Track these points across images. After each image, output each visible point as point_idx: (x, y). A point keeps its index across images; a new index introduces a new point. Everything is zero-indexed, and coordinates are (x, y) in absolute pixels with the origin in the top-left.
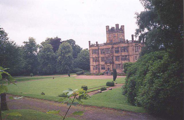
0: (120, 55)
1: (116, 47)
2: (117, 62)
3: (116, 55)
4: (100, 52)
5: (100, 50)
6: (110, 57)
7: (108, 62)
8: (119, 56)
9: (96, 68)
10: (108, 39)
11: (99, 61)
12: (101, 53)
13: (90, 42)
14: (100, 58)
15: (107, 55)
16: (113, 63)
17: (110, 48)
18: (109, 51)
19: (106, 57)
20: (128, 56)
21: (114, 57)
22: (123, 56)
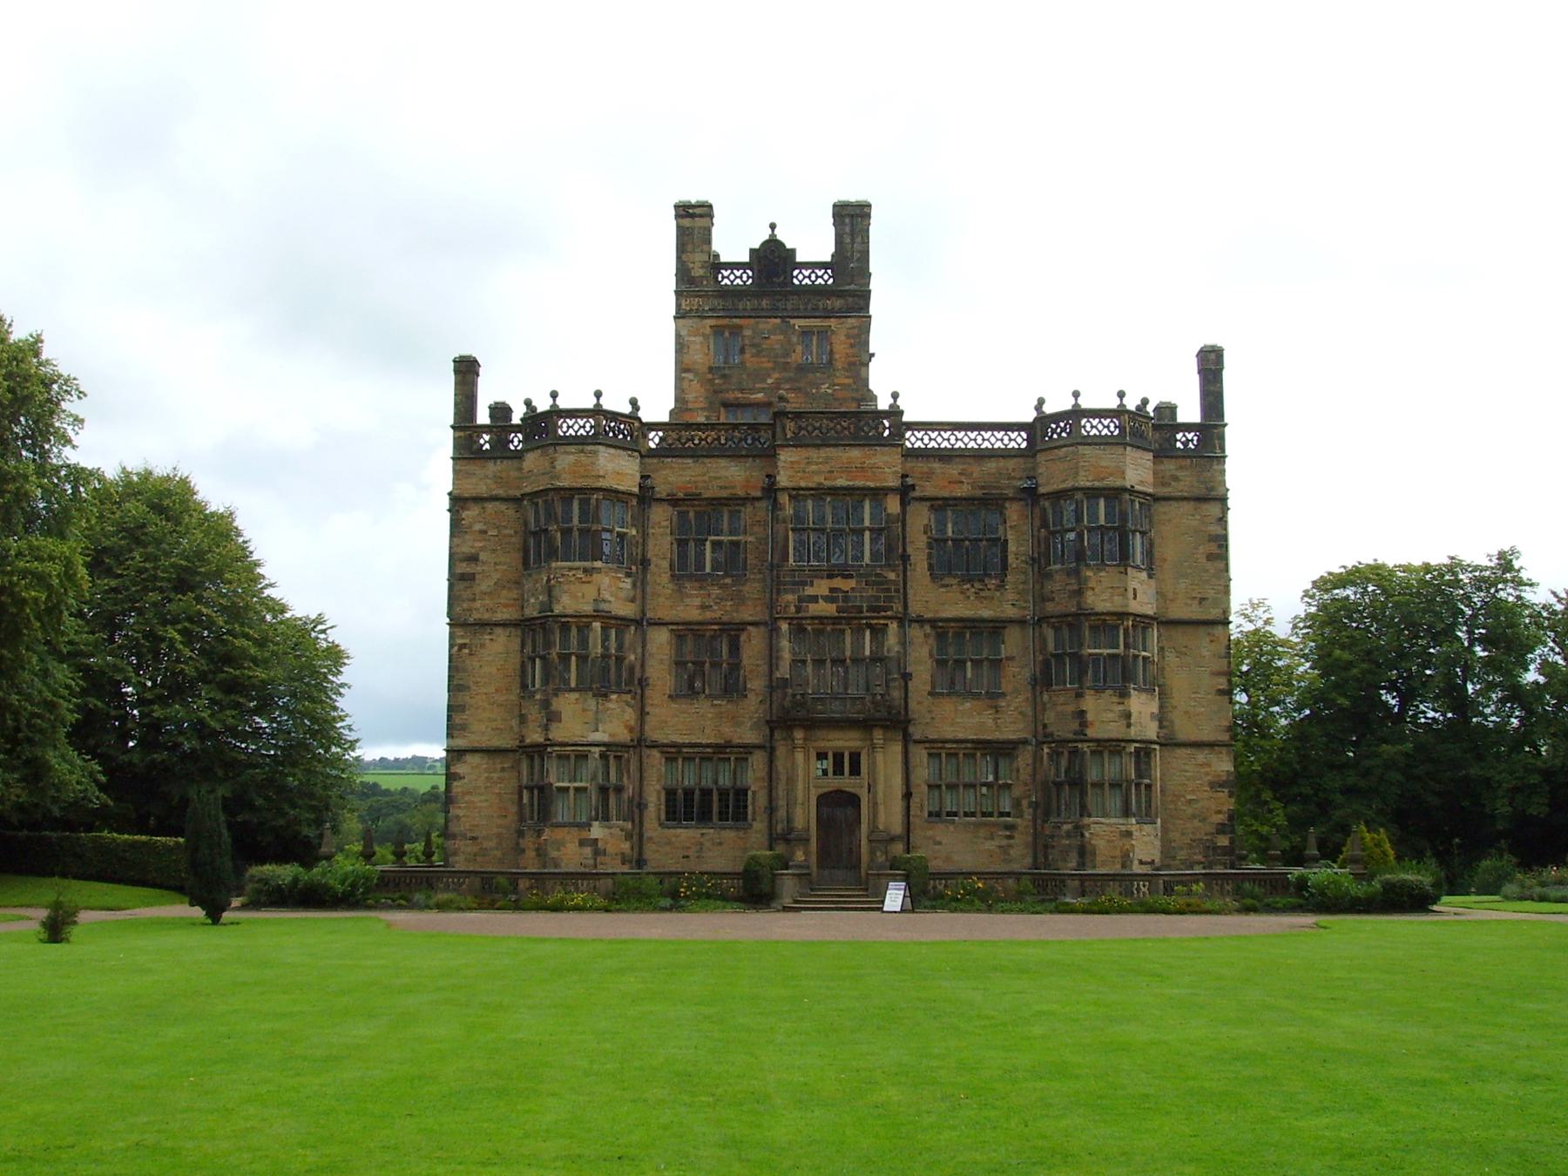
0: (1011, 612)
1: (963, 491)
2: (961, 720)
3: (955, 603)
4: (661, 546)
5: (661, 516)
6: (878, 632)
7: (835, 710)
8: (996, 628)
9: (604, 790)
10: (696, 393)
11: (636, 685)
12: (684, 571)
13: (466, 370)
14: (660, 639)
15: (821, 587)
16: (897, 722)
17: (877, 494)
18: (861, 532)
19: (798, 630)
20: (1154, 633)
21: (915, 632)
22: (1108, 624)
